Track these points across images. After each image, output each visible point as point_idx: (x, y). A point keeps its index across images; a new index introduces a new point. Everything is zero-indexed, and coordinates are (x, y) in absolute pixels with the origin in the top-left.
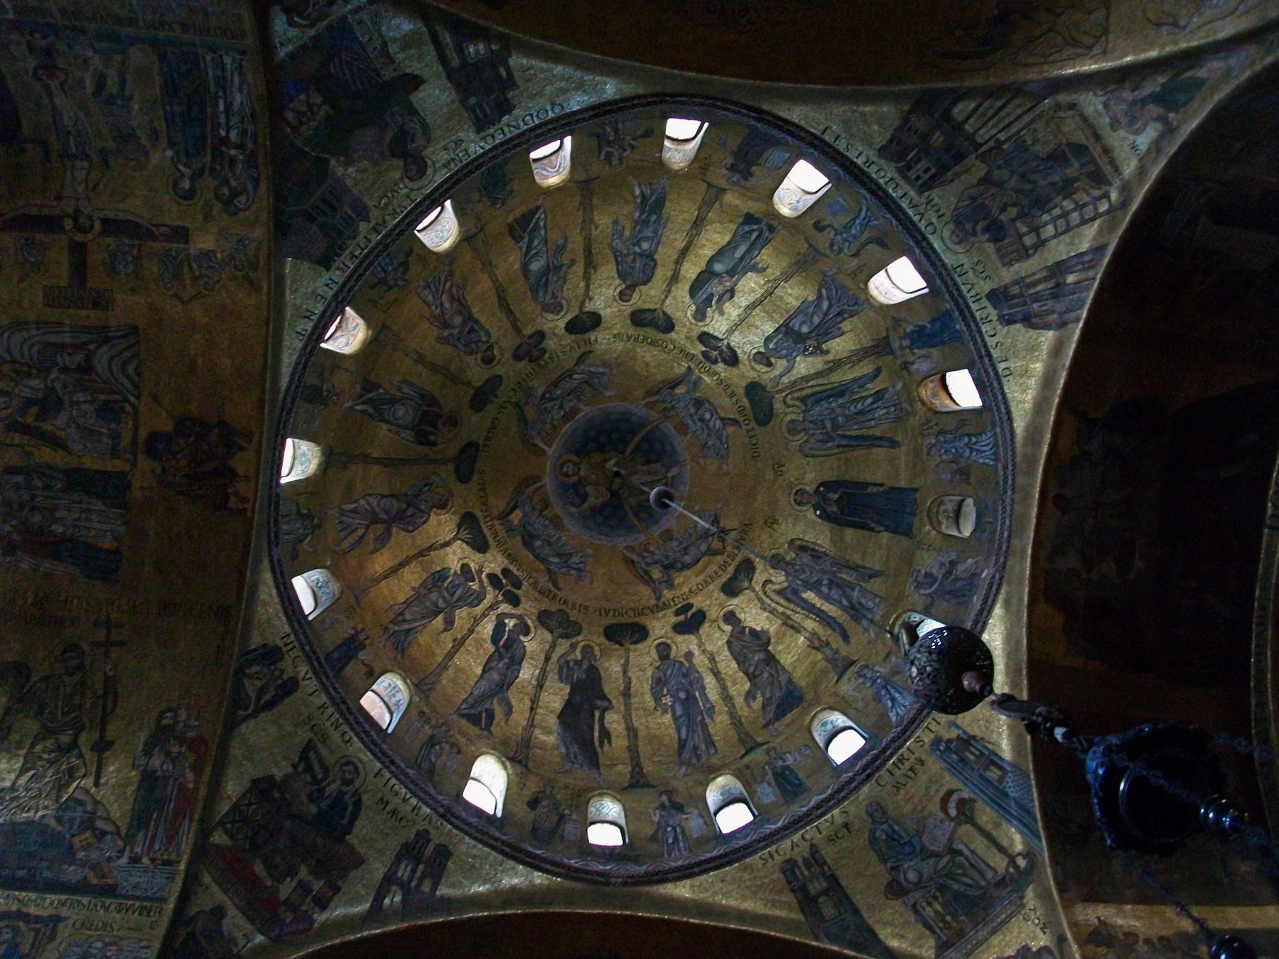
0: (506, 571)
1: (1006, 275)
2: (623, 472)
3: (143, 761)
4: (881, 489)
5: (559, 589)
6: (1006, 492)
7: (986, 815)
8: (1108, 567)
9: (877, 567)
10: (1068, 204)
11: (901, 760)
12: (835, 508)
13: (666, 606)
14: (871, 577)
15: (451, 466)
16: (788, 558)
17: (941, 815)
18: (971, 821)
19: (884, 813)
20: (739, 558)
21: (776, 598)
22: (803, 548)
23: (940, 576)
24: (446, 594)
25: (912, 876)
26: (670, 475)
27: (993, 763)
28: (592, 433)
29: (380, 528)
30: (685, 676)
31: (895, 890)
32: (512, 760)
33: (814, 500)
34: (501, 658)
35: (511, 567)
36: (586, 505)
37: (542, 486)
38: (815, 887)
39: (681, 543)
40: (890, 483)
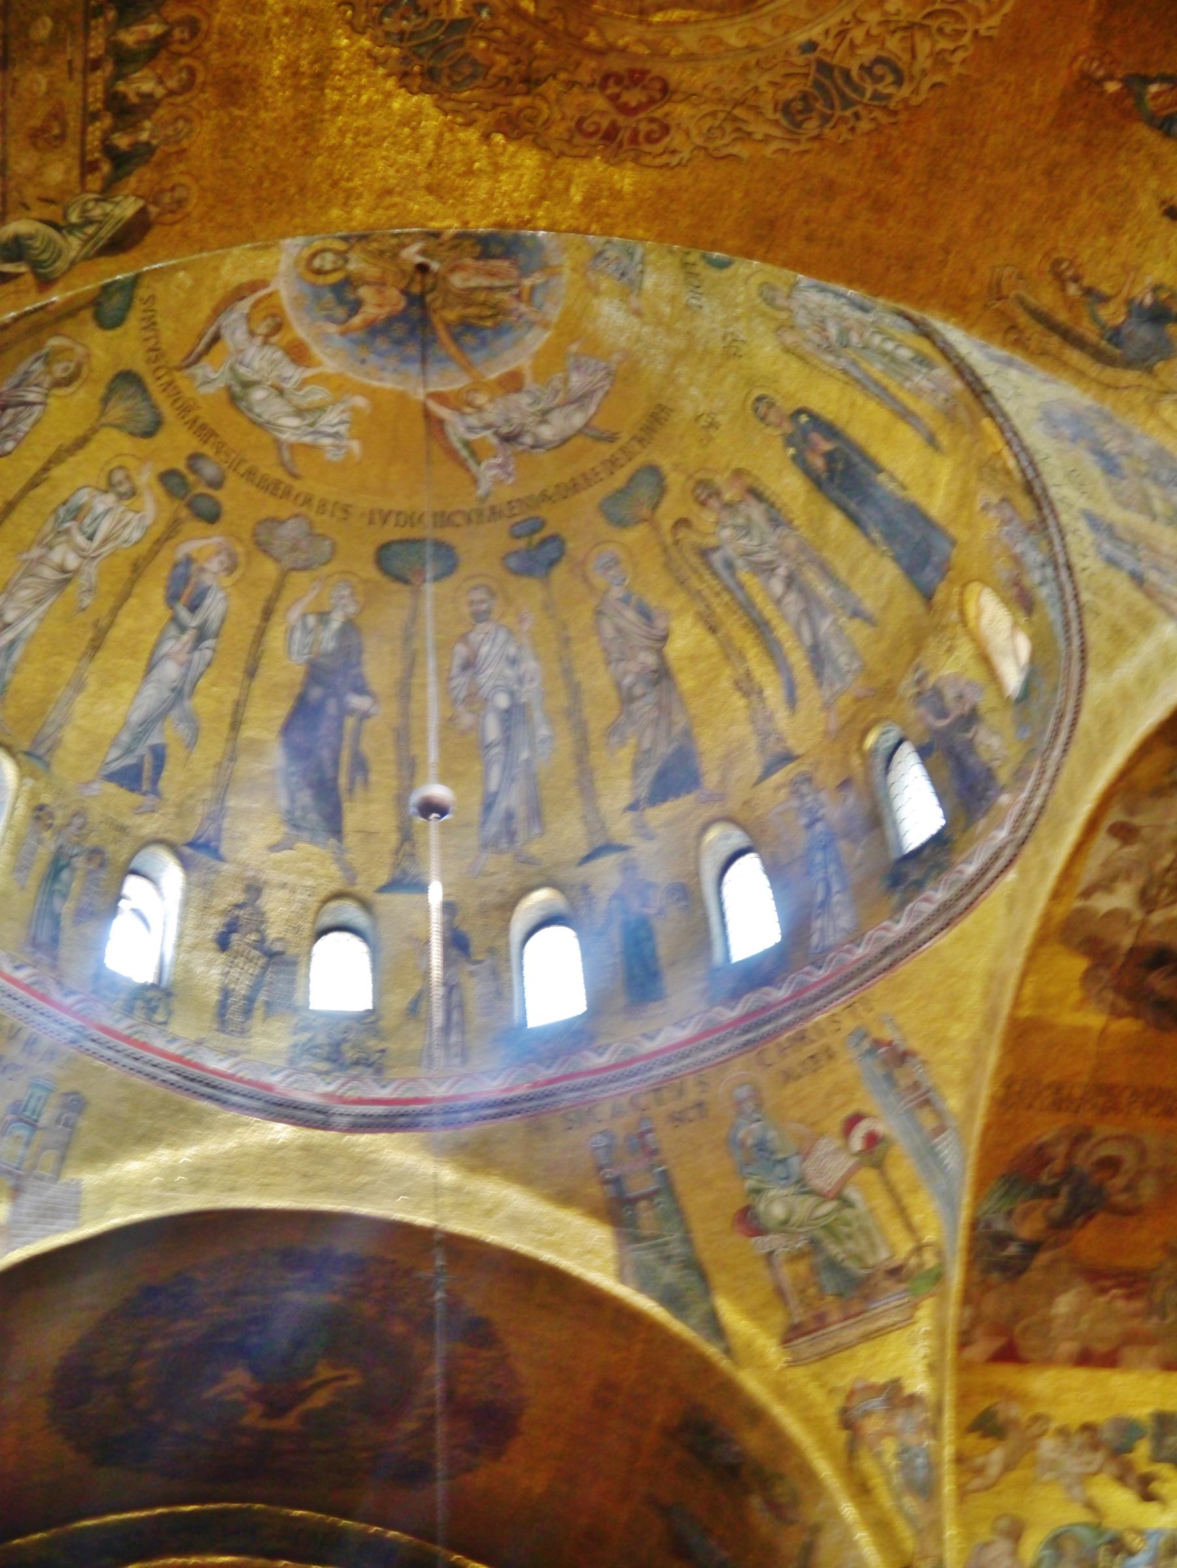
0: (194, 459)
1: (1116, 515)
2: (435, 266)
4: (901, 493)
5: (296, 476)
6: (1051, 746)
7: (903, 1169)
9: (869, 605)
11: (801, 1038)
12: (819, 463)
14: (856, 614)
15: (87, 314)
16: (727, 496)
17: (838, 1142)
18: (878, 1166)
19: (759, 1106)
21: (695, 560)
22: (756, 494)
23: (955, 713)
24: (80, 540)
26: (527, 282)
27: (927, 1102)
33: (788, 427)
34: (183, 629)
35: (208, 450)
36: (357, 320)
37: (270, 295)
38: (640, 1183)
39: (536, 401)
40: (916, 494)
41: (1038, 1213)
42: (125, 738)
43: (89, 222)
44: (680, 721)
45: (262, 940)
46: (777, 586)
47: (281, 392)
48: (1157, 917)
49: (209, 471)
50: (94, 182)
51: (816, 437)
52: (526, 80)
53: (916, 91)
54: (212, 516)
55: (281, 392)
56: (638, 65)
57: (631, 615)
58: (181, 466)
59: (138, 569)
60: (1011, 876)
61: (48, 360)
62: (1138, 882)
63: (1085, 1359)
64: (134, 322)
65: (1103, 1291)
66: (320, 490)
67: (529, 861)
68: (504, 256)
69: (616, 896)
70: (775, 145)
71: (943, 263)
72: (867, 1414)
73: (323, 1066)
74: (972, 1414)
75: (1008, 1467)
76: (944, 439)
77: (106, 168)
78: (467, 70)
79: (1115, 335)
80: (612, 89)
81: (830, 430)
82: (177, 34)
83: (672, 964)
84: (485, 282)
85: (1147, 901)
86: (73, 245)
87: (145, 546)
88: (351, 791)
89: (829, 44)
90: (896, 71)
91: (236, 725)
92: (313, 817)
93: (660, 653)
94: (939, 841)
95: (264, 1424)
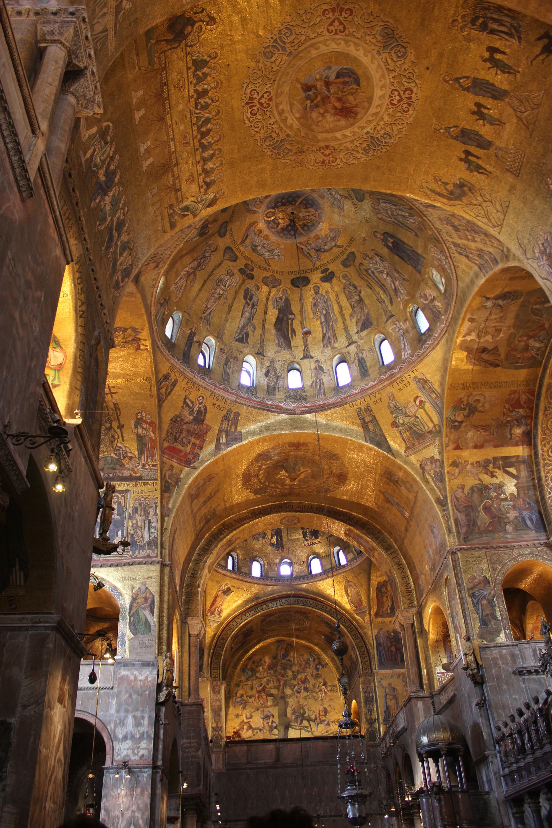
0: (246, 265)
1: (459, 241)
3: (135, 431)
8: (489, 338)
10: (486, 238)
12: (391, 245)
13: (317, 269)
14: (404, 279)
15: (217, 234)
18: (423, 408)
20: (347, 253)
21: (365, 273)
25: (401, 421)
26: (317, 213)
28: (279, 200)
29: (191, 276)
30: (325, 302)
31: (395, 424)
32: (257, 354)
34: (249, 305)
36: (279, 228)
38: (367, 419)
41: (462, 415)
42: (239, 331)
43: (203, 200)
44: (366, 311)
45: (276, 373)
46: (385, 276)
47: (264, 247)
48: (482, 340)
49: (250, 267)
50: (202, 190)
51: (389, 239)
52: (301, 152)
53: (395, 140)
54: (252, 277)
55: (264, 247)
56: (327, 144)
57: (352, 288)
58: (243, 267)
59: (236, 292)
60: (447, 335)
61: (209, 246)
62: (477, 332)
63: (476, 447)
64: (228, 235)
65: (478, 431)
66: (276, 269)
67: (335, 348)
68: (311, 207)
69: (356, 353)
70: (363, 159)
71: (408, 182)
72: (426, 465)
73: (293, 400)
74: (450, 461)
75: (459, 473)
76: (419, 234)
77: (205, 187)
78: (287, 151)
79: (451, 193)
80: (322, 151)
81: (392, 236)
82: (217, 152)
83: (370, 367)
84: (307, 214)
85: (479, 336)
86: (200, 206)
87: (238, 286)
88: (292, 337)
89: (372, 132)
90: (389, 135)
91: (263, 325)
92: (284, 344)
93: (359, 296)
94: (429, 330)
95: (291, 483)
